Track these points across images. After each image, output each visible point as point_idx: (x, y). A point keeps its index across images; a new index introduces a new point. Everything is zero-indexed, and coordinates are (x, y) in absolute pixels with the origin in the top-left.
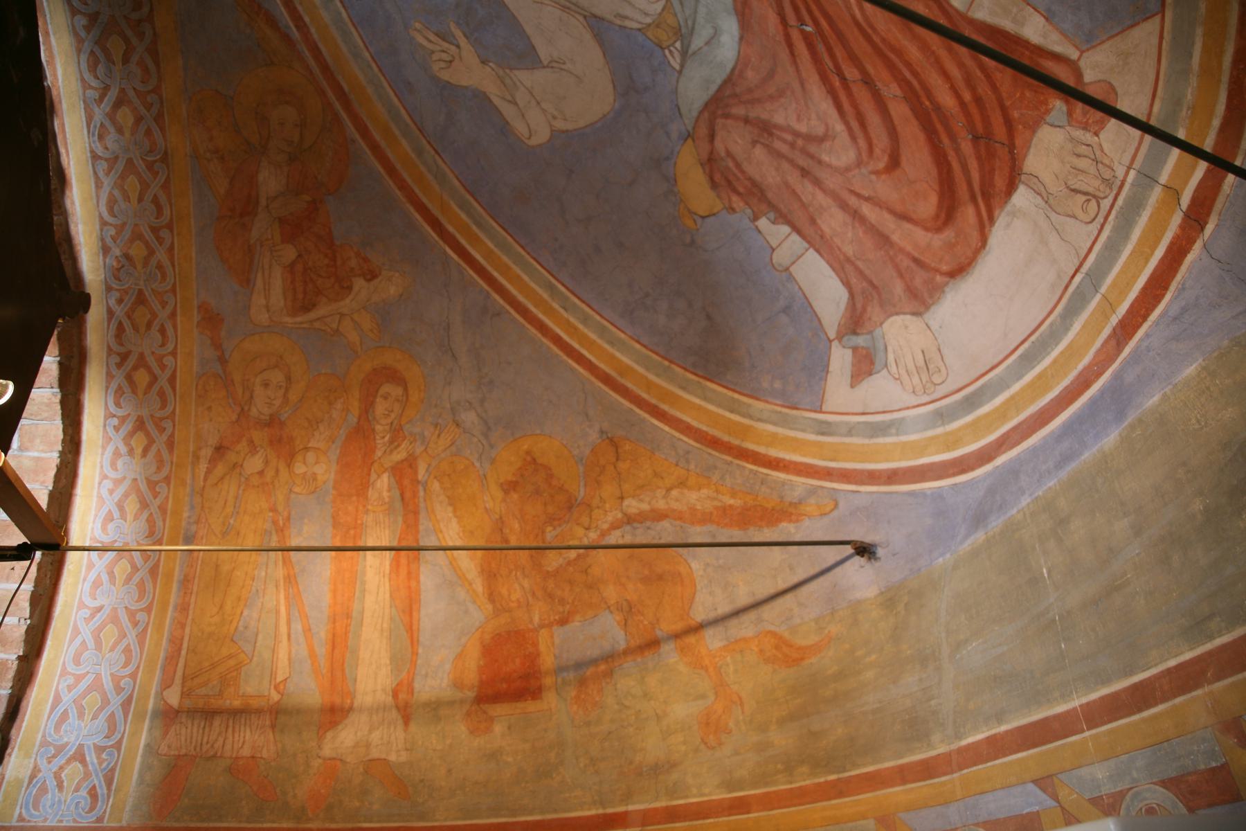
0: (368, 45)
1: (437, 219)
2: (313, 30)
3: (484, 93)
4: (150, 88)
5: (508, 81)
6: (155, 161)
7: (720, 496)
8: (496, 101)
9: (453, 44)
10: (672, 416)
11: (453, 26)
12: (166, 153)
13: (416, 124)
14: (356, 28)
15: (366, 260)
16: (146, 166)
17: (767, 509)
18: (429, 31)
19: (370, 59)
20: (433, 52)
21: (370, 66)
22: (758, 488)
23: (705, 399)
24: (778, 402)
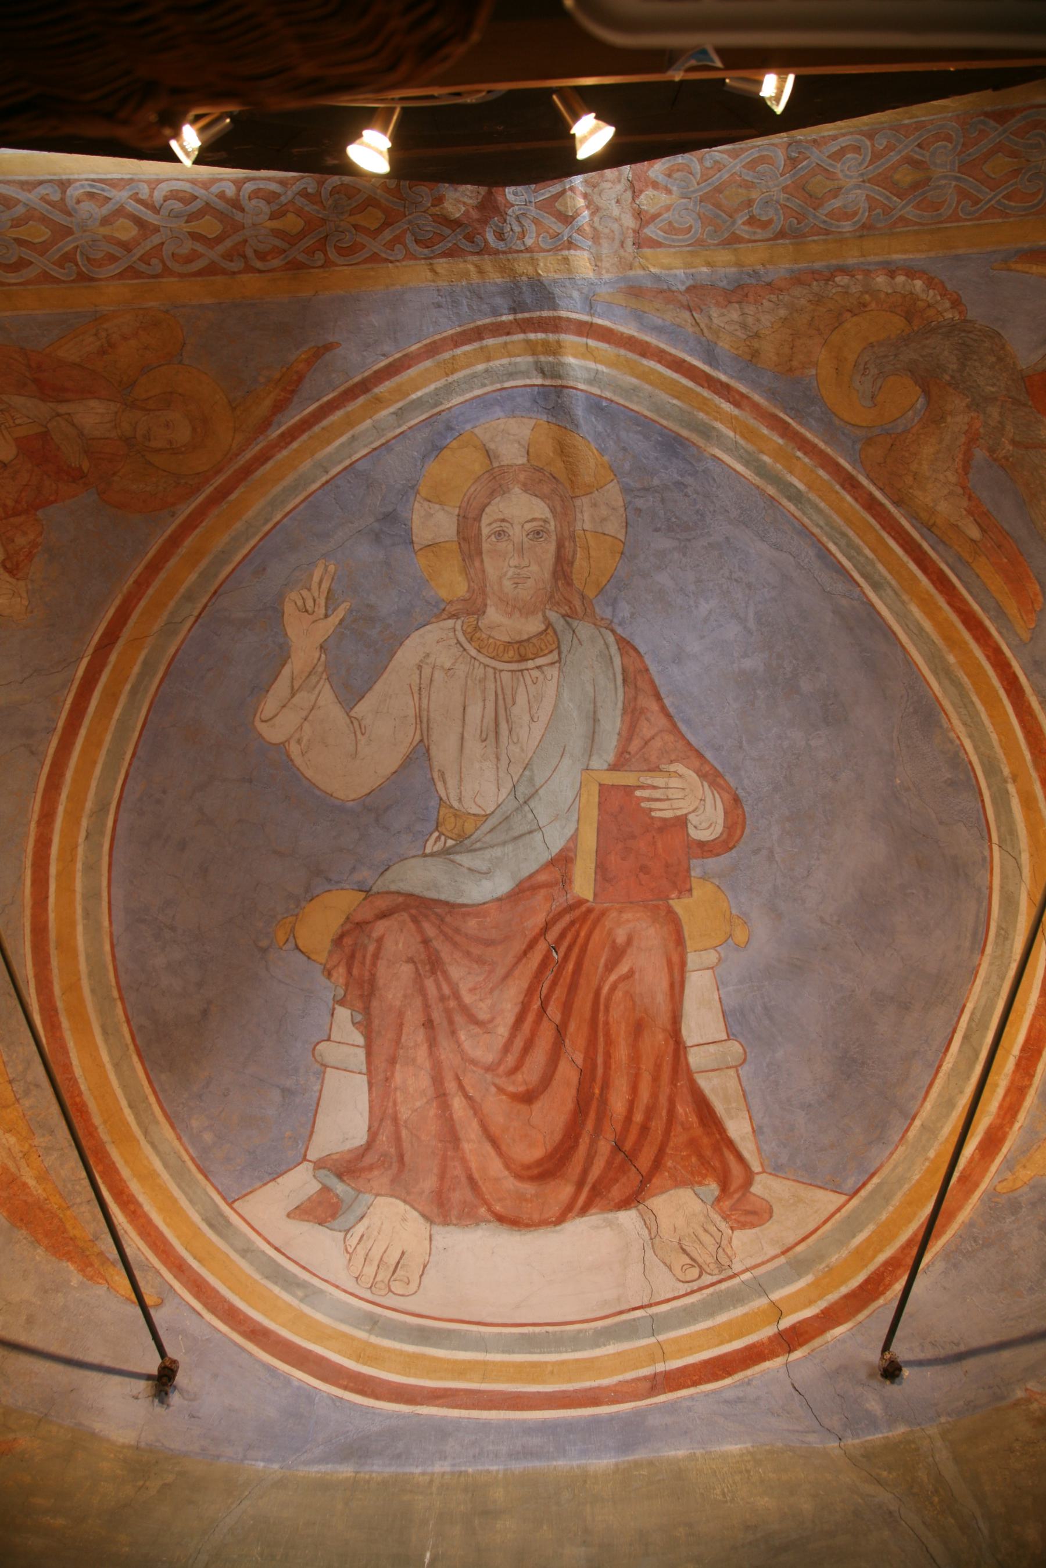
0: (291, 515)
1: (118, 638)
2: (285, 453)
3: (289, 657)
4: (169, 264)
5: (314, 679)
6: (77, 265)
7: (23, 1163)
8: (286, 671)
9: (326, 610)
10: (62, 1038)
11: (346, 605)
12: (92, 279)
13: (221, 585)
14: (302, 502)
15: (30, 556)
16: (67, 253)
17: (65, 1231)
18: (330, 581)
19: (275, 520)
20: (309, 590)
21: (267, 521)
22: (78, 1200)
23: (116, 1066)
24: (191, 1151)
